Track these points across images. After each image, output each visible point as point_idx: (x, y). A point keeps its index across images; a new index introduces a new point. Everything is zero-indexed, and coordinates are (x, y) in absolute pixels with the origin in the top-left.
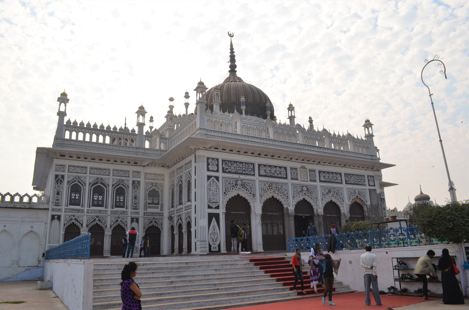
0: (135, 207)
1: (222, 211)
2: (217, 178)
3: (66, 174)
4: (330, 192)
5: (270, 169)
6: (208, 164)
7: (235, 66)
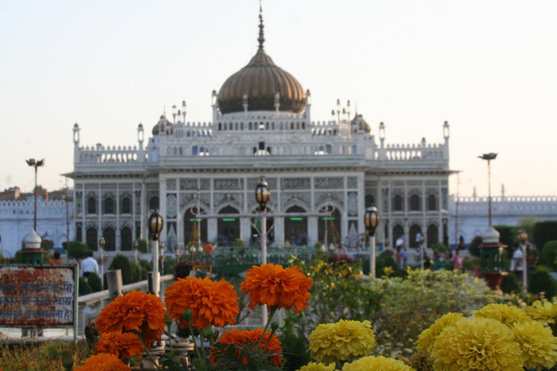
0: (139, 213)
1: (180, 219)
3: (83, 190)
5: (225, 182)
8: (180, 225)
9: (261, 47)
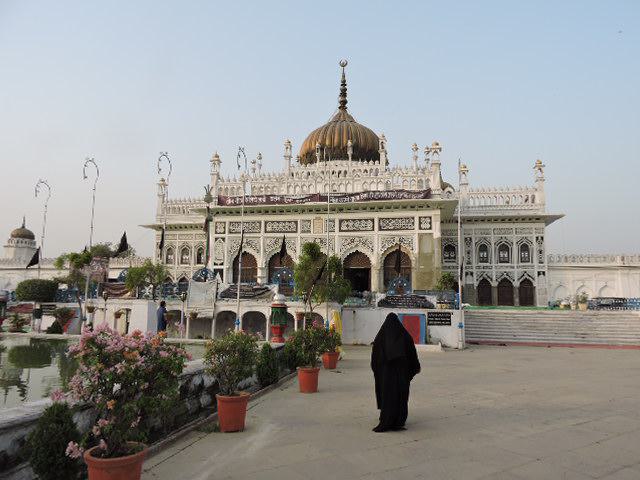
2: (224, 239)
6: (216, 227)
8: (227, 273)
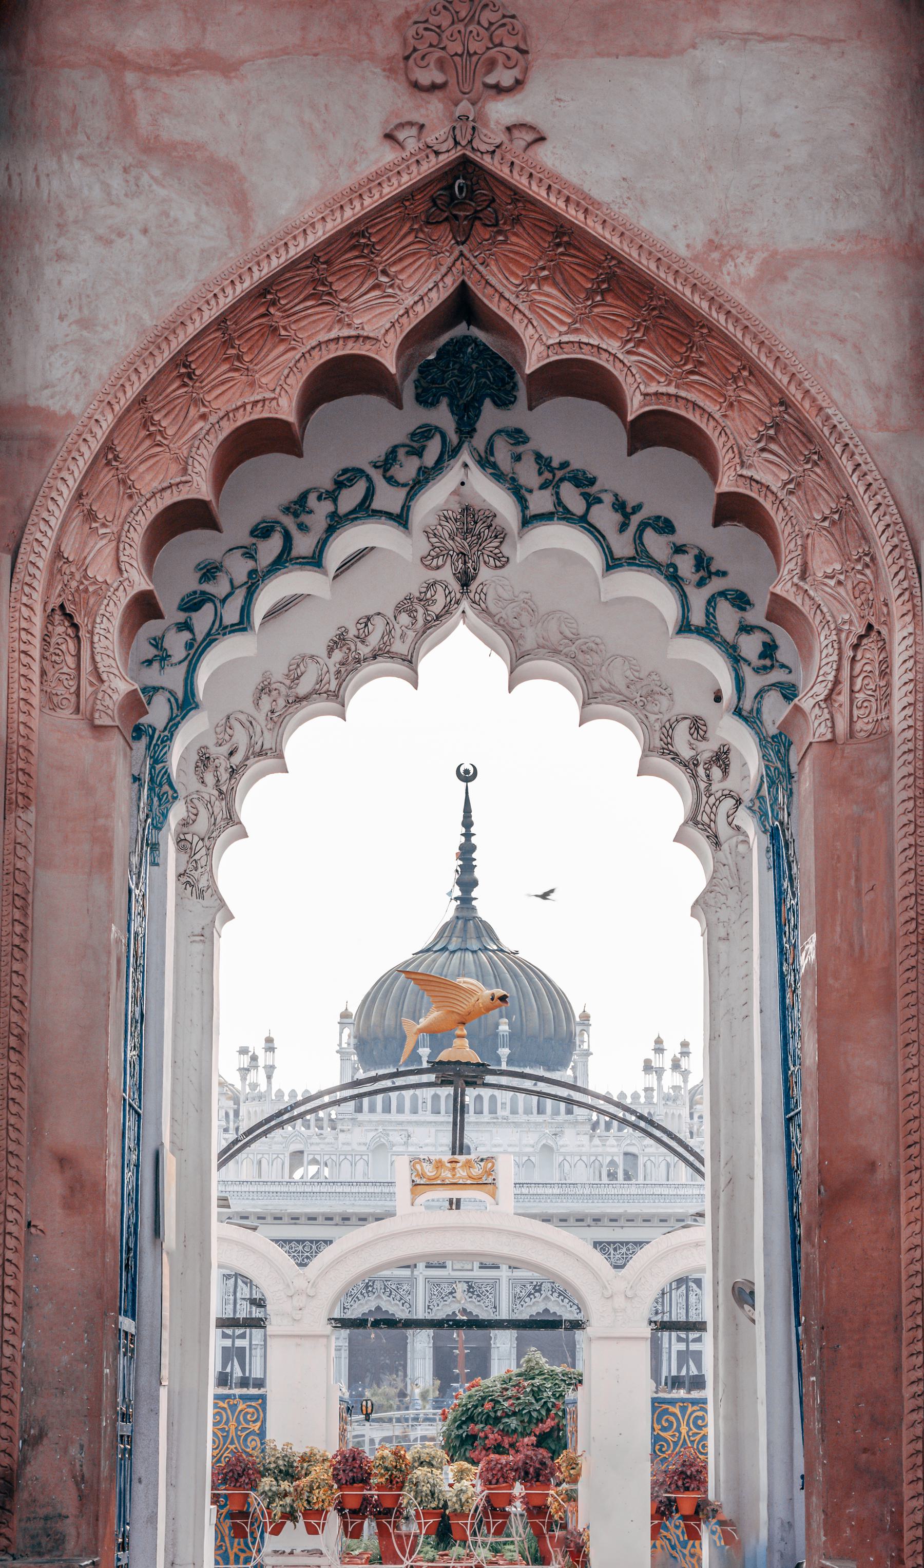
4: (539, 1291)
7: (475, 883)
9: (466, 901)
